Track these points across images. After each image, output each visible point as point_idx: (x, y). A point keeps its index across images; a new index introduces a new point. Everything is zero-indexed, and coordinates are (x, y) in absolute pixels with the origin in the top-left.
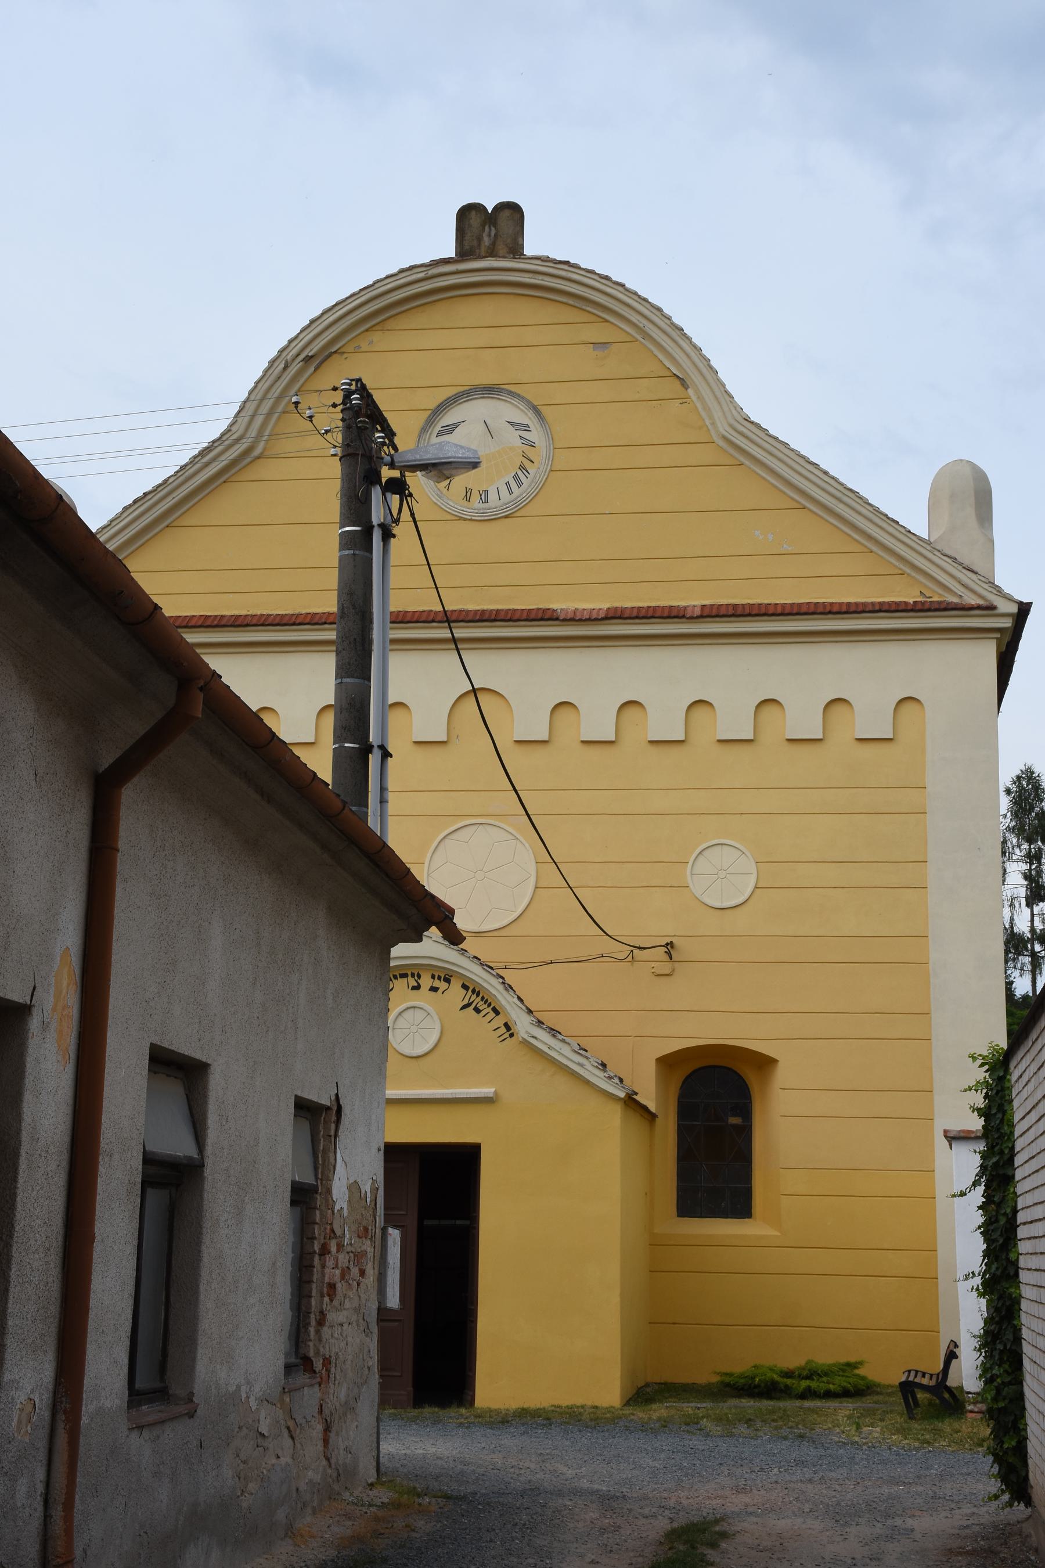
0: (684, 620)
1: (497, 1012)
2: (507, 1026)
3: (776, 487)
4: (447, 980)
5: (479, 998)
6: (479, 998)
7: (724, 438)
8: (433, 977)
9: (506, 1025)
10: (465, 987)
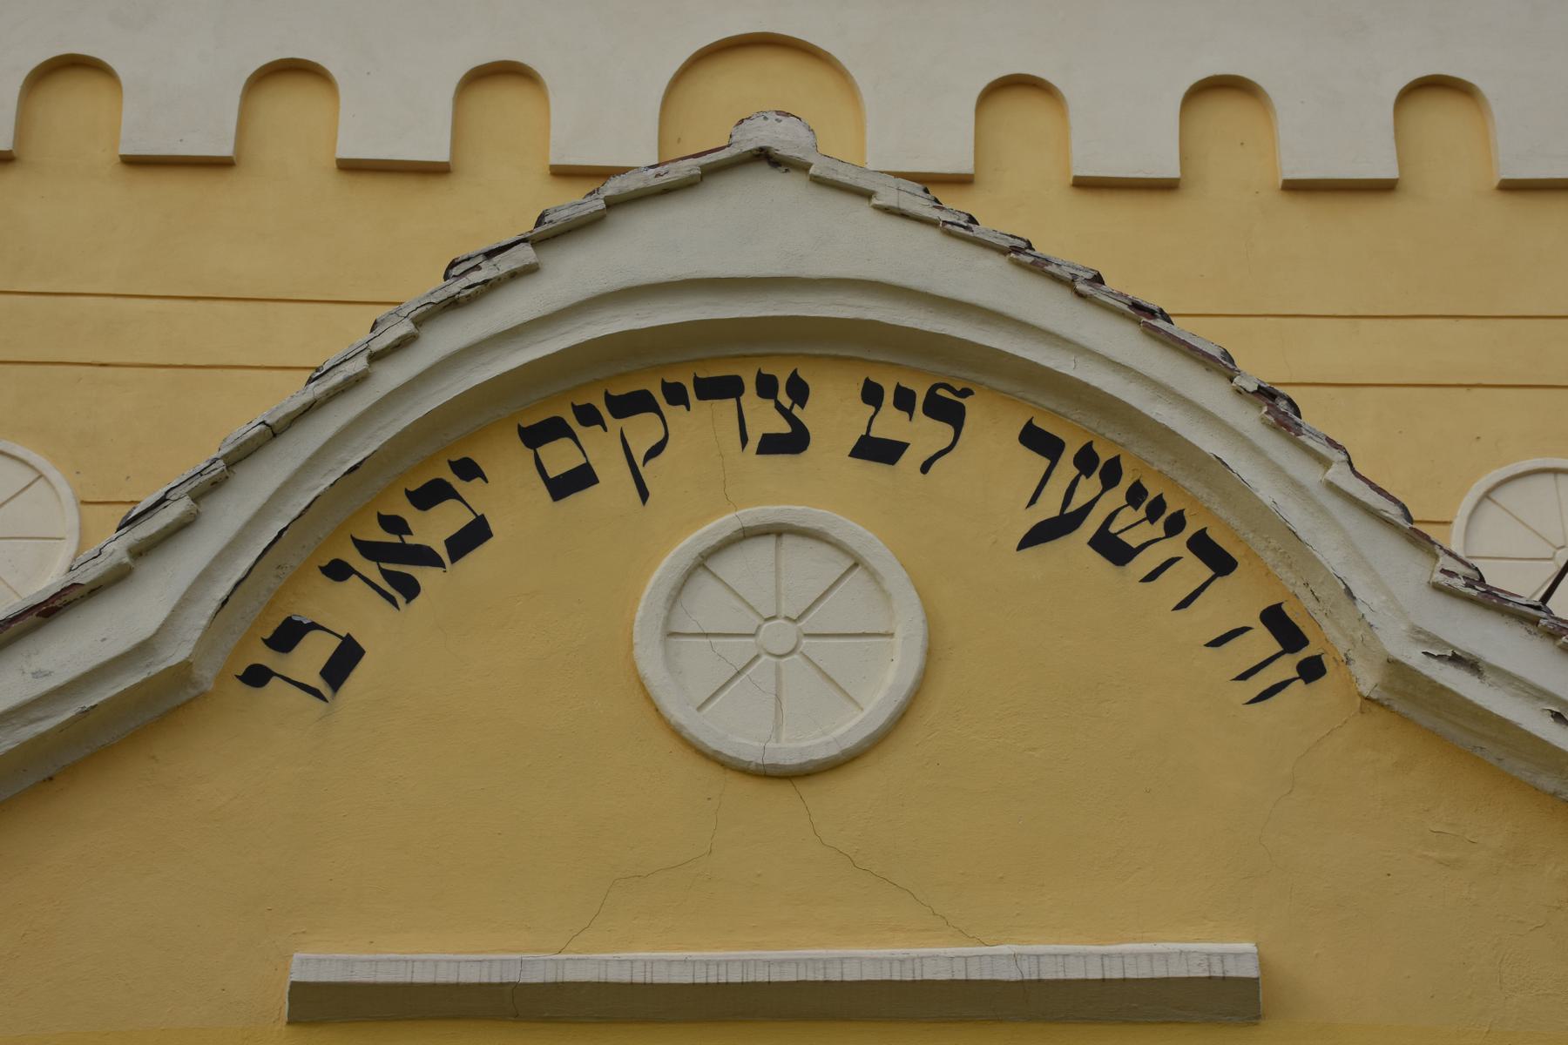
1: (1220, 562)
4: (947, 411)
5: (1117, 496)
6: (1117, 496)
8: (872, 394)
9: (1275, 619)
10: (1037, 440)
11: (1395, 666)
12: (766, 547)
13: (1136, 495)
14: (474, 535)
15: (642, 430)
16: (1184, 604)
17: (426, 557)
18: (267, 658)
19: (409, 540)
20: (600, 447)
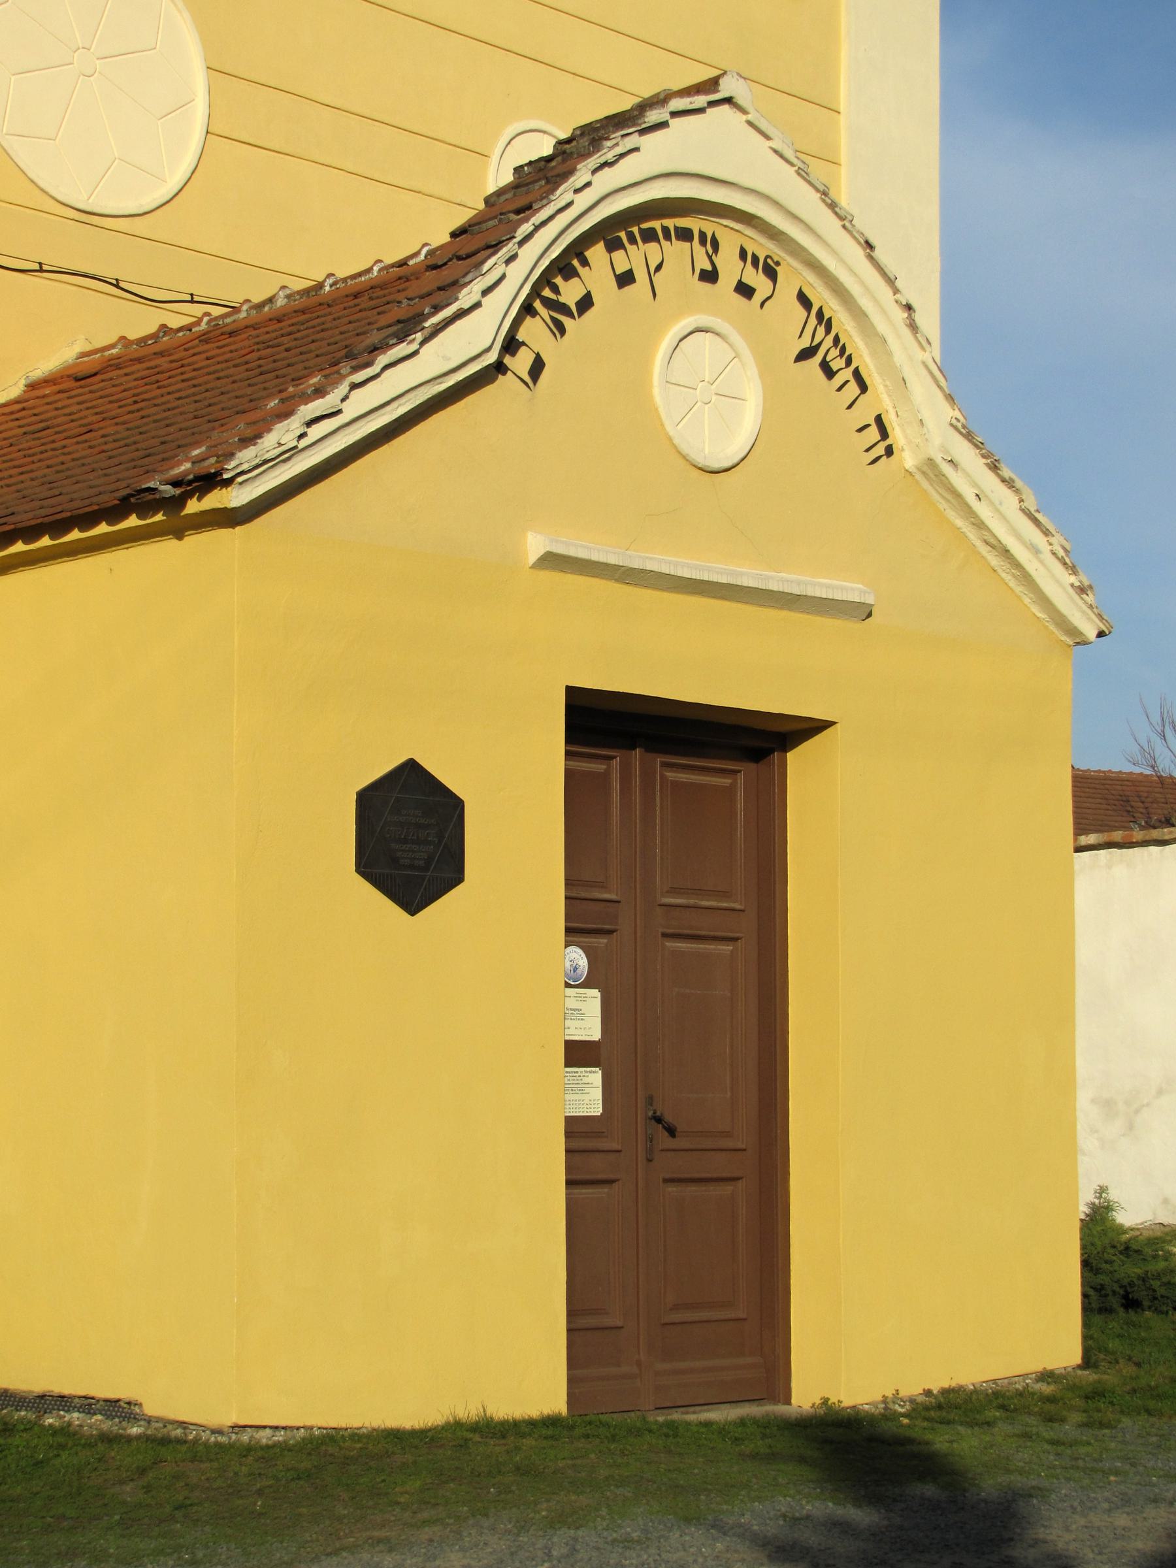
4: (771, 273)
8: (743, 254)
11: (931, 462)
13: (837, 340)
14: (586, 303)
16: (850, 407)
19: (562, 299)
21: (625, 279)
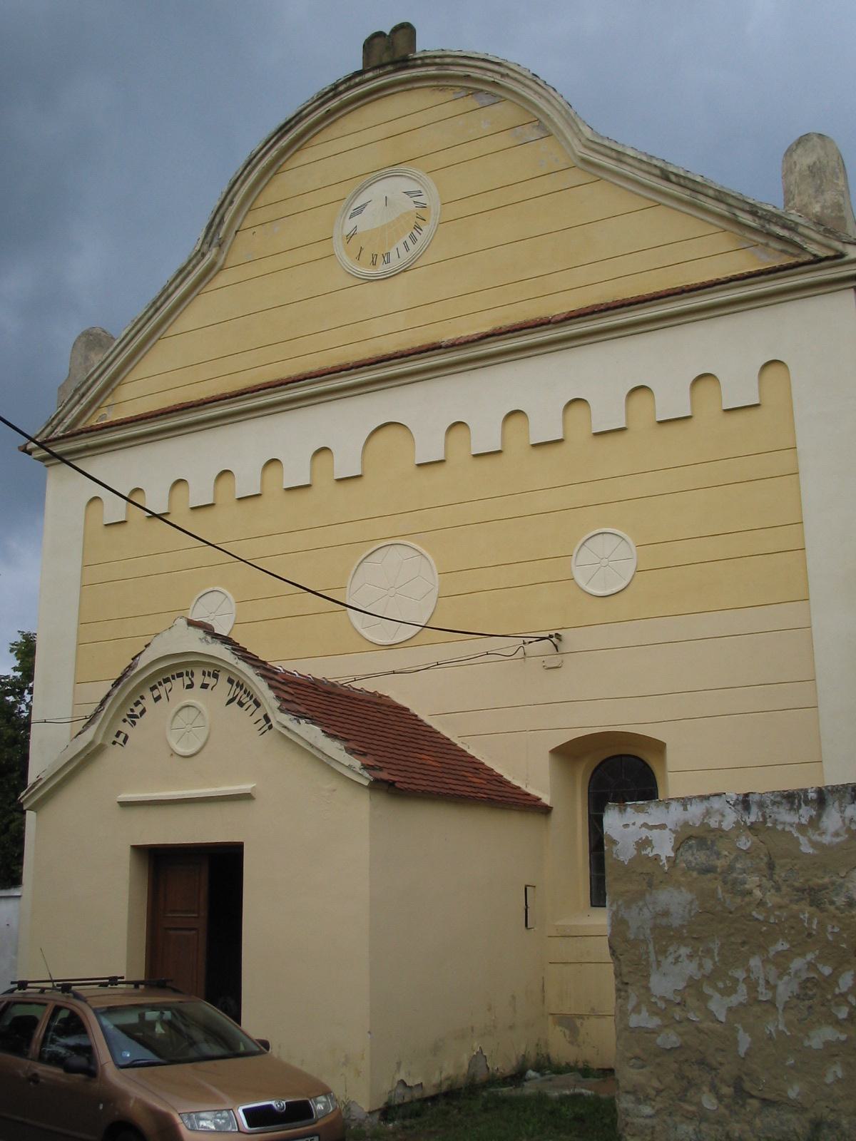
0: (550, 326)
1: (258, 704)
2: (267, 718)
3: (633, 192)
4: (216, 676)
7: (584, 160)
8: (204, 674)
10: (231, 681)
12: (187, 709)
15: (168, 685)
17: (136, 717)
18: (116, 739)
20: (161, 690)
21: (157, 699)
